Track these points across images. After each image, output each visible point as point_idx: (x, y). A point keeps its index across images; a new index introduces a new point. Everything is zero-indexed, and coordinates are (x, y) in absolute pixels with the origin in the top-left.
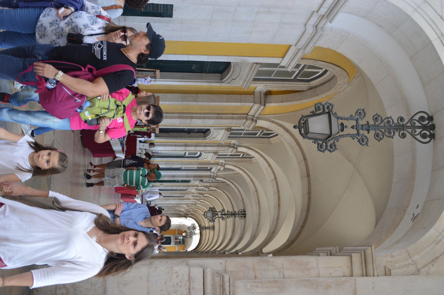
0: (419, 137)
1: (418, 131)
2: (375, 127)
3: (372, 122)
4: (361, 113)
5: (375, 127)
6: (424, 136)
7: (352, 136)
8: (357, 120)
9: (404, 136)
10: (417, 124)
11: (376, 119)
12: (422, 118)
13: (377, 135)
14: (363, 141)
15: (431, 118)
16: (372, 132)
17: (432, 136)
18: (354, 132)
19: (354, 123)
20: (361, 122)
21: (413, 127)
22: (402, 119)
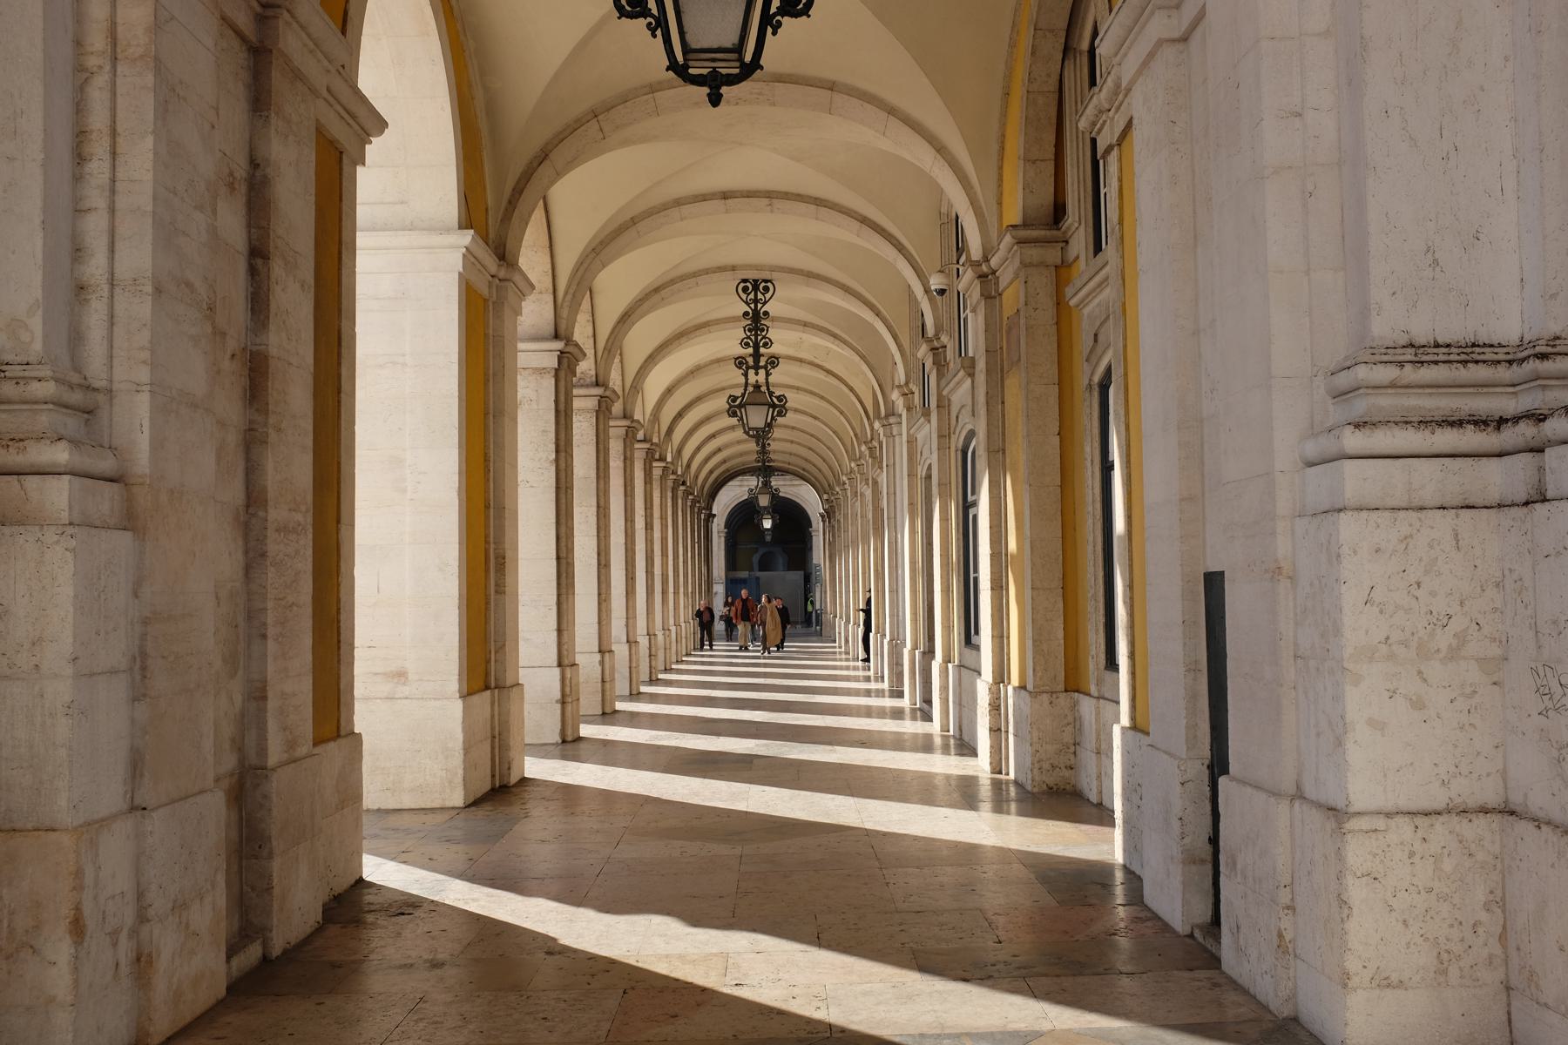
0: (768, 296)
1: (760, 296)
2: (756, 347)
3: (750, 350)
4: (740, 362)
5: (756, 347)
6: (766, 289)
7: (768, 374)
8: (748, 368)
9: (766, 313)
10: (752, 296)
11: (747, 344)
12: (745, 290)
13: (765, 345)
14: (774, 361)
15: (745, 281)
16: (762, 350)
17: (766, 281)
18: (762, 372)
19: (751, 372)
20: (750, 361)
21: (756, 301)
22: (746, 314)
